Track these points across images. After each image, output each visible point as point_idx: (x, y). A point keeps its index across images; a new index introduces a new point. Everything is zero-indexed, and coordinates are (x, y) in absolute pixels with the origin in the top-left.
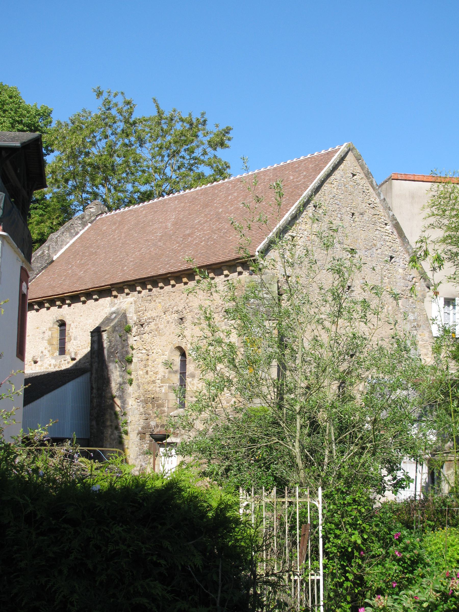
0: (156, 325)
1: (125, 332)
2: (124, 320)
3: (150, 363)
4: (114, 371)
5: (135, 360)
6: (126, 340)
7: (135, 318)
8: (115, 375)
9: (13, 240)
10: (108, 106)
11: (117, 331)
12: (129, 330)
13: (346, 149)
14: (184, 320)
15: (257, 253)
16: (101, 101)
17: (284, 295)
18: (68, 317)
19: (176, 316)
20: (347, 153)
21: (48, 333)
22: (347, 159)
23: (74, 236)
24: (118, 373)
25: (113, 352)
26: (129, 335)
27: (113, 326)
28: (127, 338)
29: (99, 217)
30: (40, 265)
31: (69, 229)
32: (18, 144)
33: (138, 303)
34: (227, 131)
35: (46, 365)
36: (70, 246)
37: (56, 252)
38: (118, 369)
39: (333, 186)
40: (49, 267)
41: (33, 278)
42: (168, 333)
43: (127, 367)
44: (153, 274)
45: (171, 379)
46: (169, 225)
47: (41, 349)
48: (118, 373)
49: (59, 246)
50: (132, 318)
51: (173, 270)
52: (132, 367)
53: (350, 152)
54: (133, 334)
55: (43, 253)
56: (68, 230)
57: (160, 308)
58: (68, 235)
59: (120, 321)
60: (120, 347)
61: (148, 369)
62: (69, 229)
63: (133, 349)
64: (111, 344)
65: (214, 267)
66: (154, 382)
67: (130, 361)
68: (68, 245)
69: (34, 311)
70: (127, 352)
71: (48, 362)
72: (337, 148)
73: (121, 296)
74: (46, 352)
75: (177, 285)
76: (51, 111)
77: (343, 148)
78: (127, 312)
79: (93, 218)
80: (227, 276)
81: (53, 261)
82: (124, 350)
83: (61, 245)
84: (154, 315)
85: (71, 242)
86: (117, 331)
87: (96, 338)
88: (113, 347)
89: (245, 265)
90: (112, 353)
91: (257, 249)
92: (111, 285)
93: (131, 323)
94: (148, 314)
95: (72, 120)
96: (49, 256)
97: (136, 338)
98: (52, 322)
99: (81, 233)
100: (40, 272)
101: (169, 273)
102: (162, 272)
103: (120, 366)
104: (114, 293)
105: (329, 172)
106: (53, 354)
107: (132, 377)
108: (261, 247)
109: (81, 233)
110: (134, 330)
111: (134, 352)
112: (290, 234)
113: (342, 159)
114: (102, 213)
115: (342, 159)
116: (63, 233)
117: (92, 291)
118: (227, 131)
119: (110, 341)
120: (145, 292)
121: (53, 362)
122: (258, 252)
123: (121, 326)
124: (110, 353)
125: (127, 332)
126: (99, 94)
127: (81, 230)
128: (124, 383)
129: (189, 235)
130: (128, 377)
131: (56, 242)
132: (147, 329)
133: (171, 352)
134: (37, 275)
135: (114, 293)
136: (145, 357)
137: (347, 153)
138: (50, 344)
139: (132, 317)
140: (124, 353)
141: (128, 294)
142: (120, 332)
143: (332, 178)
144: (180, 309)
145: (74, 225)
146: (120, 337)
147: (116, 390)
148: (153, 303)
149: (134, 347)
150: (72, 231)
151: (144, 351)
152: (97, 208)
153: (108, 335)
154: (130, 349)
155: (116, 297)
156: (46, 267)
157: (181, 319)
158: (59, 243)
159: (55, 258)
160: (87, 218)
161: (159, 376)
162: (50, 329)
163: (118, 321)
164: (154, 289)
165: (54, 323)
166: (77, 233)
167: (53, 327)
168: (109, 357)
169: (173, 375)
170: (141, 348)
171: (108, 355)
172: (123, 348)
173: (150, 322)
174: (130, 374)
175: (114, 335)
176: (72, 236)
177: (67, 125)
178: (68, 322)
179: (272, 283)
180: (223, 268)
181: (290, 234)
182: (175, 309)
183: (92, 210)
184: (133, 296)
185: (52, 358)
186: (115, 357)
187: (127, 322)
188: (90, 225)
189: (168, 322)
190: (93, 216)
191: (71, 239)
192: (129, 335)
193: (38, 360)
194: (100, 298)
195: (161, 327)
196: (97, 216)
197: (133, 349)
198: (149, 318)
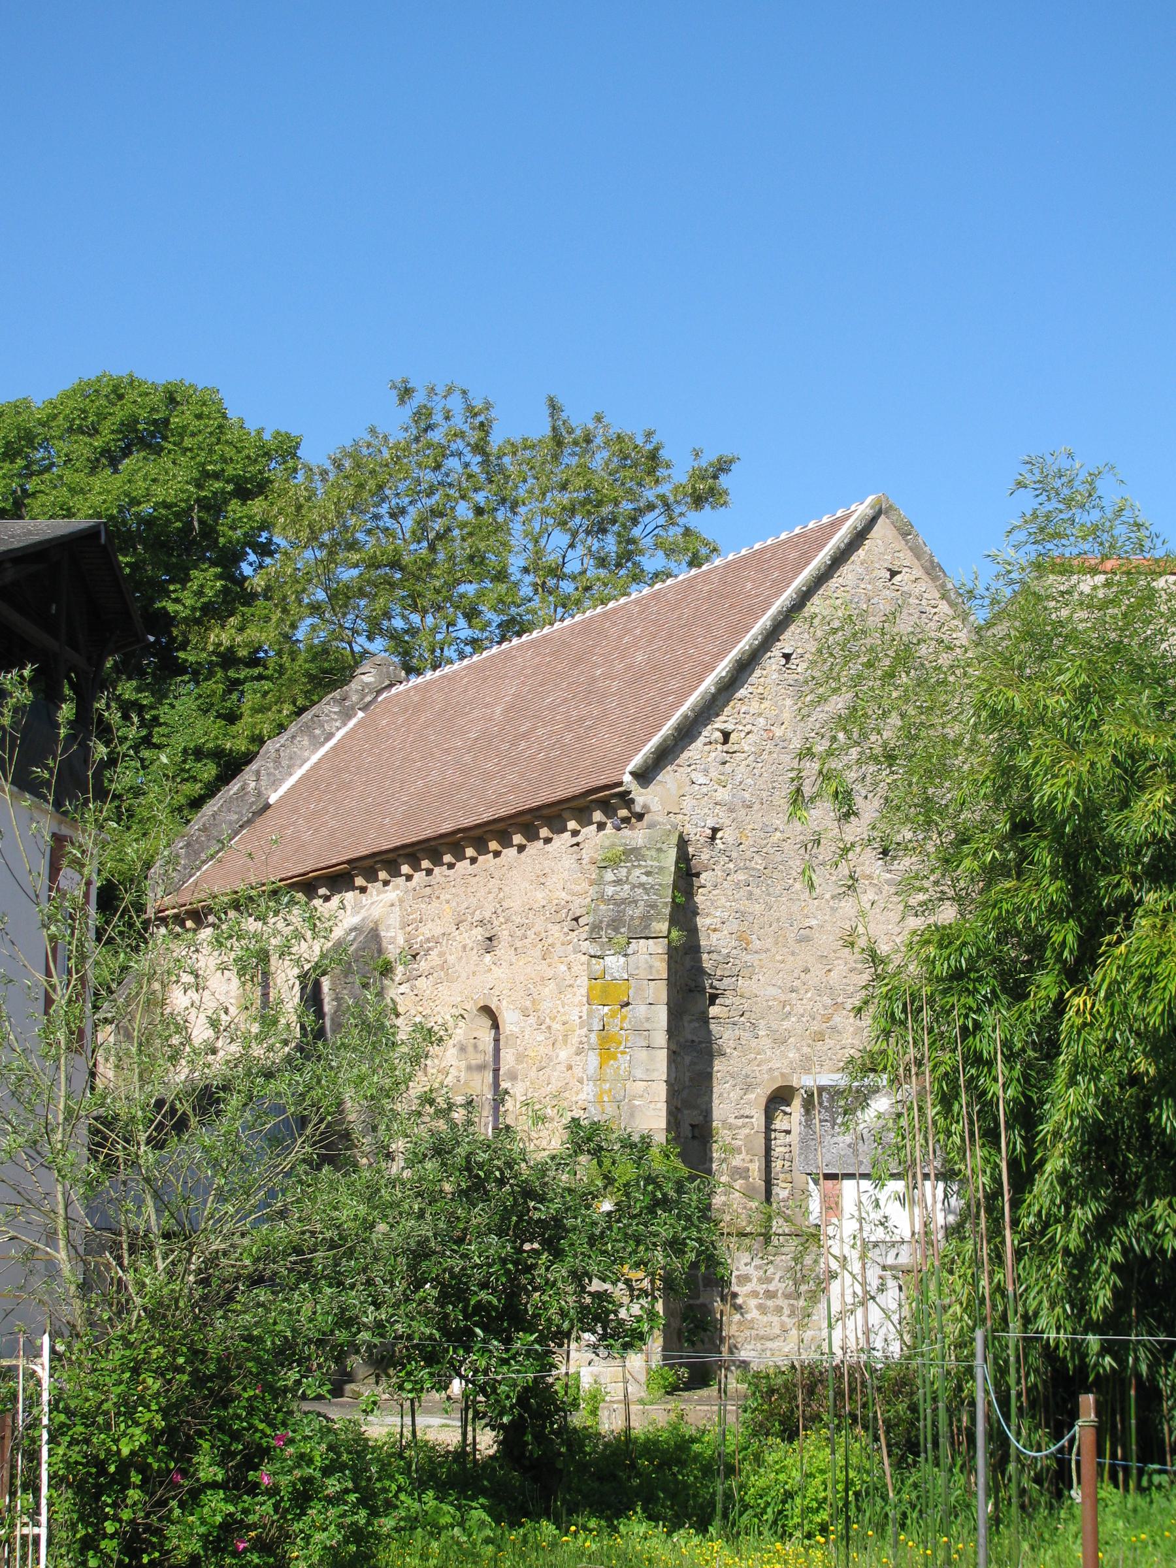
0: (441, 954)
2: (374, 947)
7: (401, 941)
10: (423, 420)
12: (387, 970)
13: (870, 512)
14: (495, 943)
15: (627, 778)
16: (405, 414)
17: (703, 876)
19: (479, 933)
20: (873, 521)
22: (873, 534)
23: (322, 744)
29: (385, 695)
30: (236, 817)
31: (308, 727)
34: (722, 467)
36: (312, 768)
37: (275, 784)
40: (259, 821)
42: (464, 975)
44: (429, 833)
46: (498, 710)
50: (394, 941)
51: (467, 822)
53: (882, 519)
54: (397, 979)
55: (243, 788)
56: (307, 729)
57: (449, 917)
58: (306, 742)
64: (339, 1005)
65: (545, 812)
68: (307, 766)
73: (373, 888)
75: (481, 858)
77: (862, 510)
78: (380, 928)
79: (368, 699)
80: (575, 833)
81: (267, 806)
83: (289, 767)
84: (438, 931)
85: (315, 758)
89: (607, 807)
91: (630, 768)
92: (349, 862)
93: (392, 952)
94: (427, 931)
95: (334, 461)
96: (259, 794)
97: (402, 989)
99: (339, 735)
100: (236, 834)
102: (446, 827)
104: (359, 881)
105: (823, 569)
108: (636, 761)
109: (339, 735)
110: (400, 970)
112: (716, 726)
113: (859, 537)
114: (391, 686)
115: (859, 537)
116: (293, 737)
117: (315, 878)
118: (722, 467)
119: (338, 999)
120: (419, 877)
122: (631, 773)
126: (406, 393)
127: (338, 729)
129: (525, 736)
131: (277, 761)
132: (423, 965)
135: (359, 881)
137: (873, 521)
139: (394, 938)
141: (386, 883)
143: (833, 583)
144: (487, 915)
148: (435, 904)
149: (401, 1010)
150: (317, 732)
153: (333, 983)
155: (363, 890)
156: (249, 822)
157: (490, 939)
158: (285, 763)
159: (272, 800)
160: (355, 698)
164: (437, 870)
166: (330, 736)
173: (430, 949)
176: (317, 744)
177: (324, 473)
179: (664, 847)
180: (566, 815)
181: (716, 726)
182: (478, 917)
183: (367, 679)
184: (397, 887)
187: (380, 951)
188: (361, 714)
189: (464, 947)
190: (370, 692)
191: (314, 752)
192: (386, 982)
195: (451, 959)
196: (379, 692)
198: (428, 940)
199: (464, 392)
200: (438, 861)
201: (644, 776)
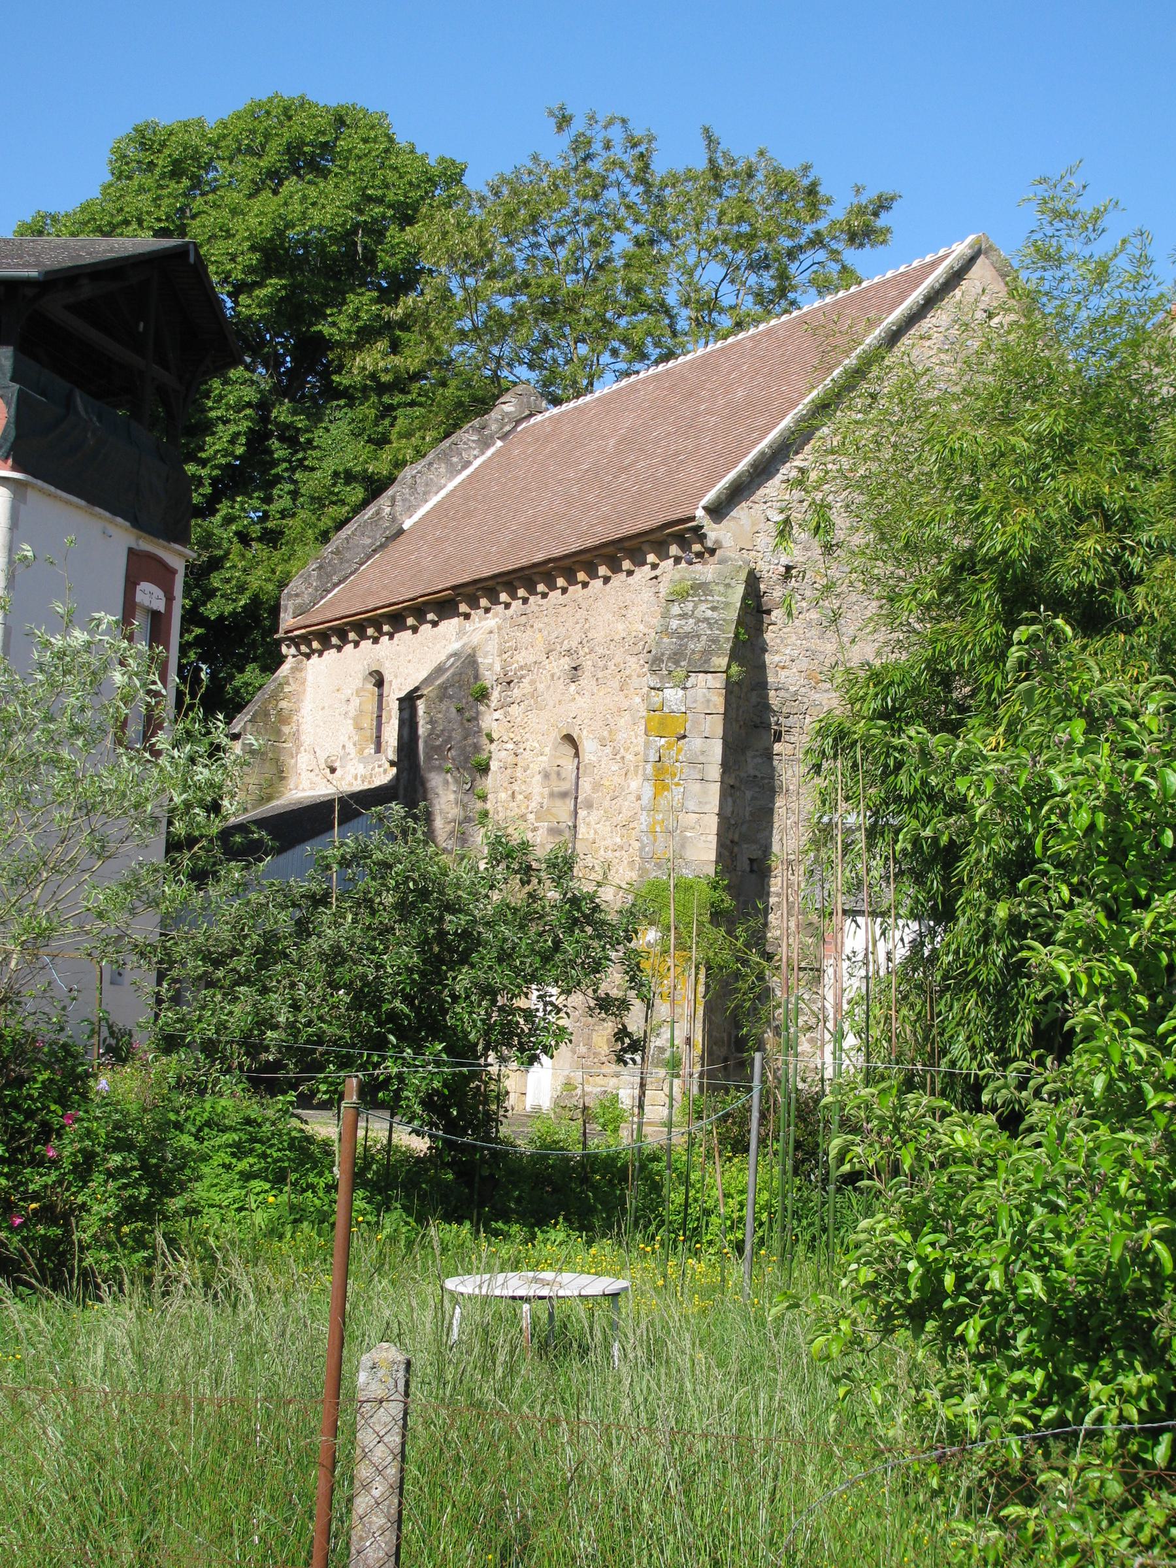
0: (532, 682)
1: (471, 699)
2: (471, 673)
3: (519, 773)
4: (440, 791)
5: (494, 765)
6: (475, 719)
7: (497, 668)
8: (443, 800)
9: (57, 487)
10: (582, 148)
11: (450, 697)
12: (483, 695)
13: (969, 252)
14: (579, 673)
15: (700, 513)
16: (564, 140)
17: (774, 613)
18: (387, 664)
19: (566, 663)
20: (971, 261)
21: (355, 702)
22: (970, 274)
23: (460, 472)
24: (452, 797)
25: (439, 747)
26: (482, 708)
27: (440, 686)
28: (478, 713)
29: (524, 425)
30: (369, 541)
31: (445, 454)
32: (33, 273)
33: (503, 632)
34: (883, 205)
35: (349, 778)
36: (448, 496)
37: (410, 510)
38: (453, 787)
39: (927, 343)
40: (393, 546)
41: (352, 573)
42: (551, 703)
43: (477, 783)
44: (524, 562)
45: (554, 810)
46: (612, 442)
47: (344, 739)
48: (452, 797)
49: (420, 497)
50: (491, 667)
51: (557, 552)
52: (489, 782)
53: (981, 260)
54: (493, 705)
55: (378, 513)
56: (445, 457)
57: (540, 645)
58: (443, 470)
59: (459, 674)
60: (457, 735)
61: (515, 787)
62: (445, 454)
63: (492, 741)
64: (433, 728)
65: (627, 544)
66: (523, 817)
67: (484, 769)
68: (443, 493)
69: (334, 650)
70: (477, 748)
71: (353, 771)
72: (941, 253)
73: (476, 615)
74: (351, 749)
75: (571, 588)
76: (463, 170)
77: (961, 249)
78: (479, 654)
79: (507, 428)
80: (654, 566)
81: (401, 532)
82: (470, 741)
83: (425, 493)
84: (532, 659)
85: (451, 486)
86: (450, 697)
87: (406, 715)
88: (438, 736)
89: (683, 541)
90: (438, 749)
91: (703, 502)
92: (453, 588)
93: (488, 678)
94: (522, 658)
95: (492, 188)
96: (394, 519)
97: (497, 715)
98: (360, 676)
99: (477, 463)
100: (369, 558)
101: (550, 560)
102: (539, 557)
103: (456, 781)
104: (463, 608)
105: (915, 308)
106: (361, 751)
107: (489, 806)
108: (710, 496)
109: (477, 463)
110: (495, 695)
111: (493, 747)
112: (796, 463)
113: (956, 277)
114: (531, 415)
115: (956, 277)
116: (430, 464)
117: (424, 603)
118: (883, 205)
119: (432, 722)
120: (516, 605)
121: (361, 770)
122: (704, 508)
123: (460, 687)
124: (432, 749)
125: (477, 699)
126: (564, 121)
127: (476, 457)
128: (467, 819)
129: (625, 469)
130: (479, 805)
131: (413, 487)
132: (516, 692)
133: (555, 749)
134: (362, 564)
135: (463, 608)
136: (511, 759)
137: (971, 261)
138: (359, 728)
139: (492, 665)
140: (469, 749)
141: (487, 610)
142: (460, 700)
143: (926, 324)
144: (574, 644)
145: (462, 446)
146: (459, 710)
147: (445, 836)
148: (529, 632)
149: (495, 736)
150: (455, 459)
151: (510, 746)
152: (521, 404)
153: (428, 707)
154: (485, 740)
155: (467, 616)
156: (383, 546)
157: (575, 669)
158: (421, 489)
159: (405, 526)
160: (494, 427)
161: (533, 805)
162: (358, 692)
163: (454, 675)
164: (532, 599)
165: (365, 679)
166: (468, 464)
167: (363, 689)
168: (429, 758)
169: (558, 803)
170: (505, 738)
171: (426, 754)
172: (465, 738)
173: (523, 677)
174: (483, 798)
175: (443, 707)
176: (454, 471)
177: (482, 199)
178: (387, 677)
179: (733, 583)
180: (645, 547)
181: (796, 463)
182: (566, 646)
183: (507, 408)
184: (496, 615)
185: (360, 761)
186: (445, 758)
187: (477, 677)
188: (499, 443)
189: (552, 676)
190: (510, 422)
191: (450, 480)
192: (482, 708)
193: (337, 764)
194: (441, 619)
195: (541, 687)
196: (518, 422)
197: (492, 741)
198: (521, 668)
199: (624, 121)
200: (532, 591)
201: (717, 511)
